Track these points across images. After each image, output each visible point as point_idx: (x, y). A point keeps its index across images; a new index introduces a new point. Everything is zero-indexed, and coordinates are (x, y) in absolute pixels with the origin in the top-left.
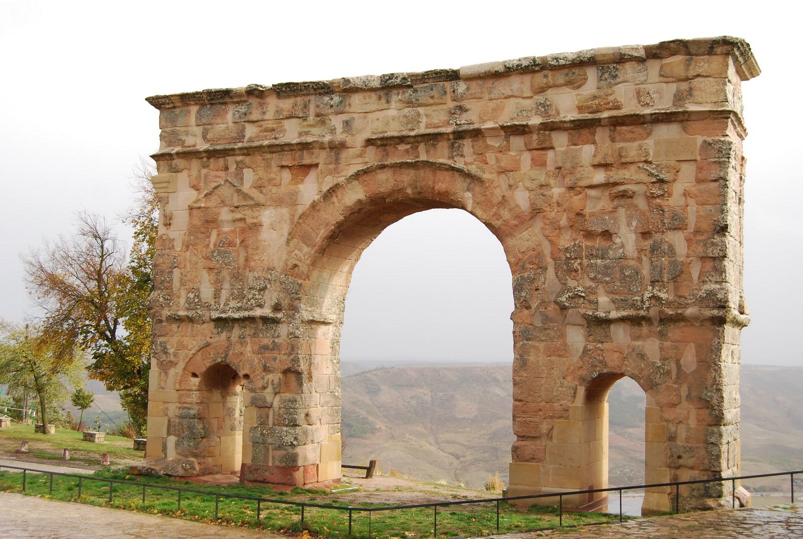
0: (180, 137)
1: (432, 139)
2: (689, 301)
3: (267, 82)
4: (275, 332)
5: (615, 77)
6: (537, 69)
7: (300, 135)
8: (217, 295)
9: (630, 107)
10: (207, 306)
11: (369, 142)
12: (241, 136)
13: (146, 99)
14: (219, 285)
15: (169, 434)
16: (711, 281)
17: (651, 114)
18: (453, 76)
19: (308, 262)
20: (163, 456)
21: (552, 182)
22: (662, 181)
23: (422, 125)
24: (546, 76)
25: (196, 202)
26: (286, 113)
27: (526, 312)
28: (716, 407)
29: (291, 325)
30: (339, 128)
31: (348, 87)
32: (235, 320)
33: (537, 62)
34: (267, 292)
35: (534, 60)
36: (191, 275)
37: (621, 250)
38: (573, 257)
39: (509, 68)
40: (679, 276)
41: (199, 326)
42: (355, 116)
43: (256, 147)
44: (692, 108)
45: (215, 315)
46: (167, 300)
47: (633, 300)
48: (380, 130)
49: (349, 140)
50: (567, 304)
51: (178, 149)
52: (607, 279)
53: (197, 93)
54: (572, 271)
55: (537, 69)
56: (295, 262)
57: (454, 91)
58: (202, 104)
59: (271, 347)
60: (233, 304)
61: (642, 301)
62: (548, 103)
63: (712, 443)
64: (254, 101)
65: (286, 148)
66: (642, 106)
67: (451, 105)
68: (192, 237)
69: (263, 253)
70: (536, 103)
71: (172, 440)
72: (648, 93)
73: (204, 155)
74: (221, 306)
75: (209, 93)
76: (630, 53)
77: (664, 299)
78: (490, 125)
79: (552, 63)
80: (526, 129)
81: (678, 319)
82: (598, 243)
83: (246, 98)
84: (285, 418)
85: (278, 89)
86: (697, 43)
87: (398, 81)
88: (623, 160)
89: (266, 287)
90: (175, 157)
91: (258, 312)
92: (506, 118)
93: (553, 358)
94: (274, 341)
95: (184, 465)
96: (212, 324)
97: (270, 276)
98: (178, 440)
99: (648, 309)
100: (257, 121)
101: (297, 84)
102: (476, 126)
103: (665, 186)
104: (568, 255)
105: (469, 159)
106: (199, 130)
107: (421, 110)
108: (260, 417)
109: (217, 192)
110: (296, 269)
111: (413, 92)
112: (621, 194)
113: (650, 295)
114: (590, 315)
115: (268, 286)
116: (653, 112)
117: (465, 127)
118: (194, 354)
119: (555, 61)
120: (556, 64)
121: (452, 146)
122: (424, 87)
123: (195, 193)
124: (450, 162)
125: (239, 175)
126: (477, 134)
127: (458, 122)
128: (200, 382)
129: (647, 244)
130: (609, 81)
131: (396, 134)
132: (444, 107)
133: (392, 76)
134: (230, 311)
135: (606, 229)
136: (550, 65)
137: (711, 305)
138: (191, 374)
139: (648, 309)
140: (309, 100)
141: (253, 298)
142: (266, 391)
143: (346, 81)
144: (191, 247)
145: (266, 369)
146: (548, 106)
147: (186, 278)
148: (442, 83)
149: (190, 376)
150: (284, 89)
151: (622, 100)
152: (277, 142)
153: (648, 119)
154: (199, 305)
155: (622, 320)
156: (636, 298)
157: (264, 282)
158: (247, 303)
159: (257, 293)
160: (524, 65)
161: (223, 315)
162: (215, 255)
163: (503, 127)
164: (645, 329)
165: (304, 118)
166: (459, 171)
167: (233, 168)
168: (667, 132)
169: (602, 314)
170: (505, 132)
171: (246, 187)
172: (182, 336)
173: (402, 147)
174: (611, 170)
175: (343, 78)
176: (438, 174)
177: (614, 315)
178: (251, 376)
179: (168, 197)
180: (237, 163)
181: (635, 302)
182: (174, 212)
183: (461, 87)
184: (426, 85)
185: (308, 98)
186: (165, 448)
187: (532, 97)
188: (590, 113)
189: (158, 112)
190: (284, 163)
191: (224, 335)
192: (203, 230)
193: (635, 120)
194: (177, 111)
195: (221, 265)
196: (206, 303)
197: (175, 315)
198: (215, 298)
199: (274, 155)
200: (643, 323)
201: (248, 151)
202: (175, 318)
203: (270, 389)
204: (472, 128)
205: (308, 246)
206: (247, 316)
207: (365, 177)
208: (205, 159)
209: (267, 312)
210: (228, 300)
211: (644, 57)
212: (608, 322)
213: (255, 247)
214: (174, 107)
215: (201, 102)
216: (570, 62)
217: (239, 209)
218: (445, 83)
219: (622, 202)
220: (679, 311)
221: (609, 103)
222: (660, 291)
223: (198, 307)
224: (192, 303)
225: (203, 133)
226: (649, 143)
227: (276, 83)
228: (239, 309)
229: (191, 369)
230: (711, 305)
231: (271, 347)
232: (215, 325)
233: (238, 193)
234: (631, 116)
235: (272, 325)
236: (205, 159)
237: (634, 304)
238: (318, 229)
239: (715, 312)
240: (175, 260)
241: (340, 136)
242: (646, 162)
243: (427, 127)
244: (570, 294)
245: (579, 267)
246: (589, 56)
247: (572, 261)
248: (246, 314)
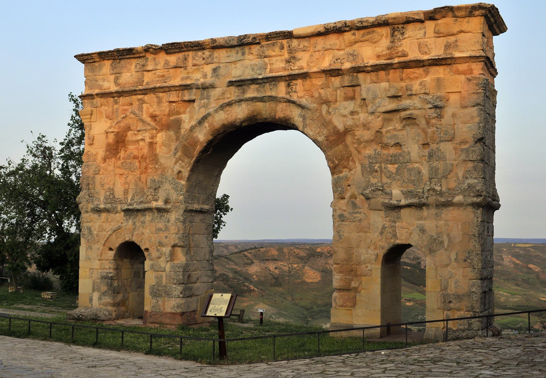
0: (98, 83)
1: (274, 80)
2: (457, 192)
3: (159, 43)
5: (403, 34)
6: (347, 29)
7: (183, 79)
8: (126, 192)
9: (414, 55)
10: (119, 201)
11: (231, 83)
12: (141, 82)
13: (75, 57)
15: (94, 291)
16: (471, 177)
17: (428, 60)
18: (288, 35)
19: (189, 169)
20: (90, 305)
21: (359, 110)
22: (436, 107)
23: (268, 70)
24: (354, 34)
25: (110, 128)
26: (172, 64)
27: (342, 201)
28: (476, 267)
29: (177, 214)
30: (209, 74)
31: (215, 45)
32: (138, 211)
33: (347, 25)
35: (345, 23)
37: (408, 157)
38: (374, 162)
39: (327, 29)
40: (449, 174)
41: (113, 215)
42: (221, 65)
43: (151, 89)
44: (457, 55)
45: (125, 207)
47: (417, 192)
48: (238, 75)
49: (217, 82)
50: (370, 196)
51: (97, 91)
52: (398, 177)
53: (110, 52)
54: (373, 172)
55: (347, 29)
56: (179, 169)
57: (289, 47)
58: (113, 59)
59: (163, 229)
60: (137, 199)
61: (423, 193)
62: (356, 53)
63: (473, 292)
64: (150, 56)
66: (422, 54)
67: (287, 56)
70: (347, 54)
71: (96, 296)
72: (427, 45)
74: (129, 201)
75: (118, 51)
76: (413, 17)
77: (438, 190)
78: (315, 69)
79: (358, 25)
80: (341, 72)
81: (447, 204)
82: (393, 151)
83: (144, 55)
84: (174, 279)
85: (166, 47)
86: (459, 8)
87: (250, 40)
88: (409, 93)
90: (95, 96)
91: (154, 204)
92: (326, 64)
93: (360, 234)
95: (104, 312)
96: (122, 213)
98: (100, 295)
99: (427, 197)
100: (152, 71)
101: (180, 43)
102: (305, 70)
103: (438, 110)
104: (371, 161)
105: (301, 94)
106: (112, 77)
107: (266, 60)
108: (157, 277)
110: (180, 174)
111: (261, 48)
112: (408, 116)
113: (428, 188)
114: (387, 203)
116: (430, 58)
117: (297, 72)
118: (110, 235)
119: (360, 23)
120: (361, 25)
121: (289, 85)
122: (268, 44)
123: (109, 122)
124: (288, 97)
125: (141, 109)
126: (305, 76)
127: (293, 68)
128: (115, 254)
129: (426, 152)
130: (398, 37)
131: (249, 77)
132: (284, 58)
133: (246, 36)
135: (398, 141)
136: (357, 26)
137: (472, 194)
138: (108, 249)
139: (427, 197)
140: (188, 55)
141: (150, 195)
142: (161, 259)
143: (213, 41)
144: (107, 160)
145: (161, 244)
146: (356, 55)
148: (280, 41)
149: (107, 250)
150: (170, 47)
151: (407, 49)
152: (165, 85)
153: (426, 63)
155: (409, 206)
156: (419, 190)
158: (146, 198)
160: (338, 27)
161: (130, 207)
162: (124, 165)
163: (324, 72)
164: (425, 212)
165: (185, 68)
166: (293, 102)
167: (136, 104)
168: (440, 72)
169: (394, 202)
170: (326, 74)
171: (145, 117)
173: (253, 87)
174: (400, 100)
175: (211, 39)
176: (279, 104)
177: (403, 202)
178: (150, 249)
180: (139, 100)
181: (418, 193)
182: (95, 136)
183: (295, 43)
184: (269, 42)
185: (187, 53)
186: (91, 300)
187: (344, 49)
188: (385, 60)
189: (83, 65)
190: (171, 100)
191: (130, 222)
193: (418, 64)
194: (97, 64)
196: (118, 199)
197: (97, 207)
198: (124, 195)
200: (424, 208)
201: (145, 92)
202: (97, 210)
203: (163, 259)
204: (302, 72)
205: (188, 158)
207: (228, 108)
209: (160, 204)
210: (133, 196)
211: (423, 19)
212: (398, 208)
214: (94, 62)
215: (113, 58)
216: (371, 24)
218: (283, 41)
219: (409, 122)
220: (449, 199)
221: (398, 52)
222: (435, 185)
224: (108, 199)
225: (114, 79)
226: (428, 79)
227: (165, 43)
228: (142, 202)
229: (109, 245)
230: (472, 194)
231: (163, 229)
234: (414, 61)
237: (417, 195)
238: (195, 146)
239: (475, 200)
240: (97, 169)
241: (209, 80)
242: (425, 93)
243: (271, 71)
244: (372, 188)
245: (378, 169)
246: (383, 19)
247: (374, 165)
248: (146, 206)
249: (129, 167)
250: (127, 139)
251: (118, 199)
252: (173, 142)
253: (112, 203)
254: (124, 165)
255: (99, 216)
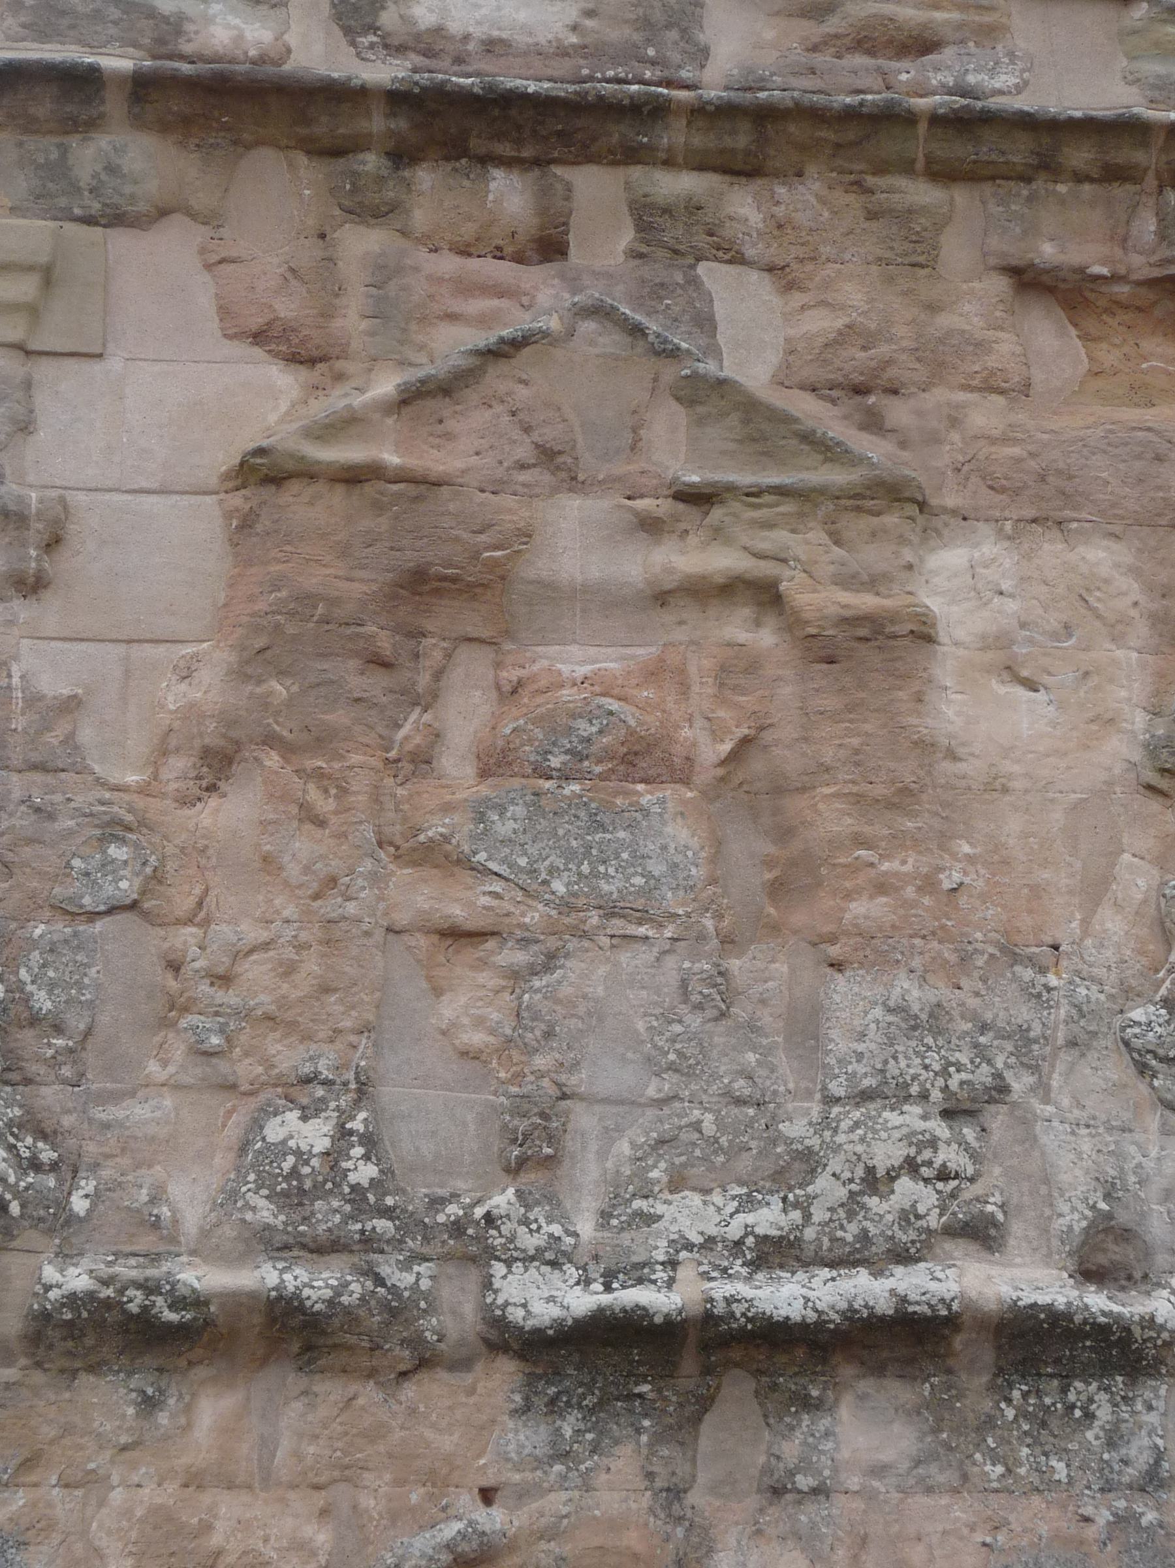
4: (1113, 1438)
10: (457, 1228)
14: (541, 1062)
34: (997, 1119)
36: (288, 970)
46: (35, 1165)
65: (1079, 156)
68: (278, 689)
69: (944, 840)
73: (377, 123)
89: (999, 1091)
90: (114, 104)
94: (1124, 1521)
97: (1024, 1013)
109: (502, 387)
115: (1020, 1083)
134: (686, 1273)
141: (911, 1166)
147: (230, 998)
154: (387, 1213)
157: (982, 1054)
158: (852, 1206)
159: (939, 1128)
172: (194, 1480)
179: (28, 385)
192: (385, 643)
195: (566, 906)
196: (437, 1203)
197: (149, 1288)
199: (961, 196)
206: (885, 1307)
208: (371, 162)
213: (879, 790)
217: (717, 514)
223: (383, 1225)
224: (318, 1191)
232: (531, 1380)
233: (689, 402)
235: (1079, 1390)
236: (371, 162)
249: (569, 855)
250: (538, 567)
251: (437, 1203)
252: (1117, 639)
253: (369, 1242)
254: (505, 828)
255: (149, 1404)
